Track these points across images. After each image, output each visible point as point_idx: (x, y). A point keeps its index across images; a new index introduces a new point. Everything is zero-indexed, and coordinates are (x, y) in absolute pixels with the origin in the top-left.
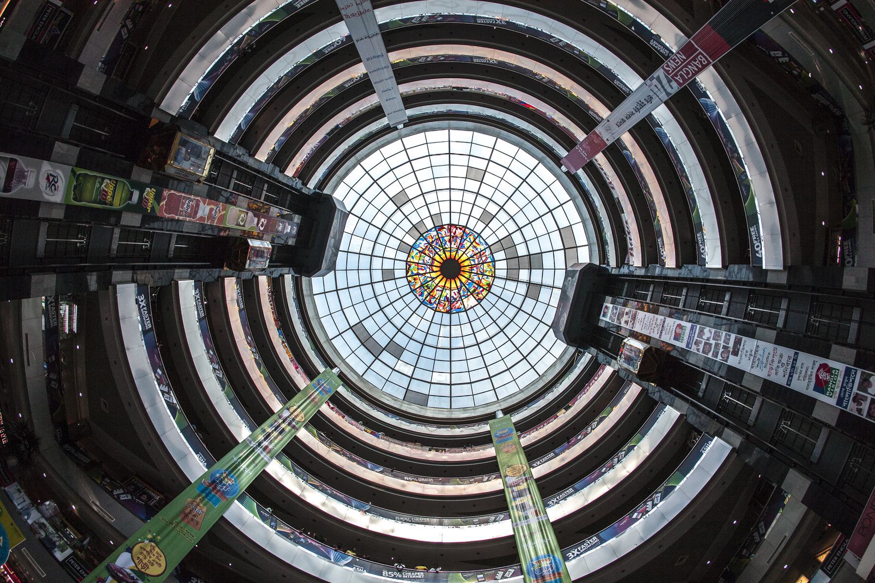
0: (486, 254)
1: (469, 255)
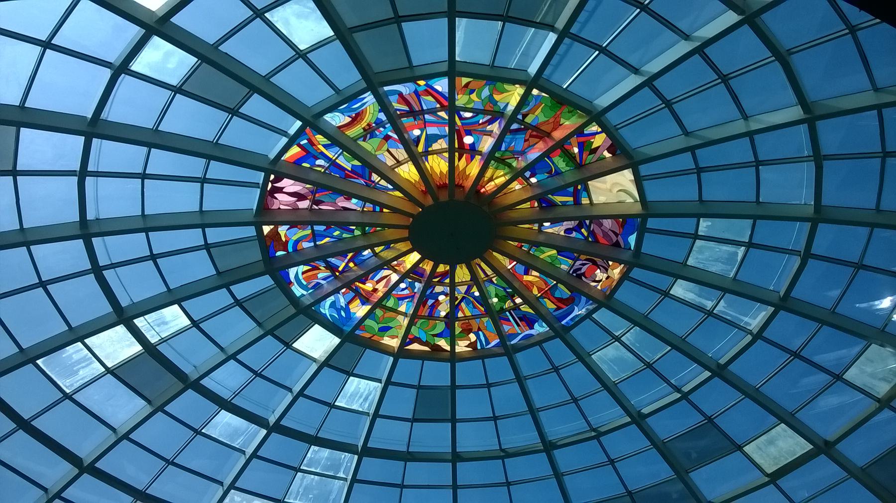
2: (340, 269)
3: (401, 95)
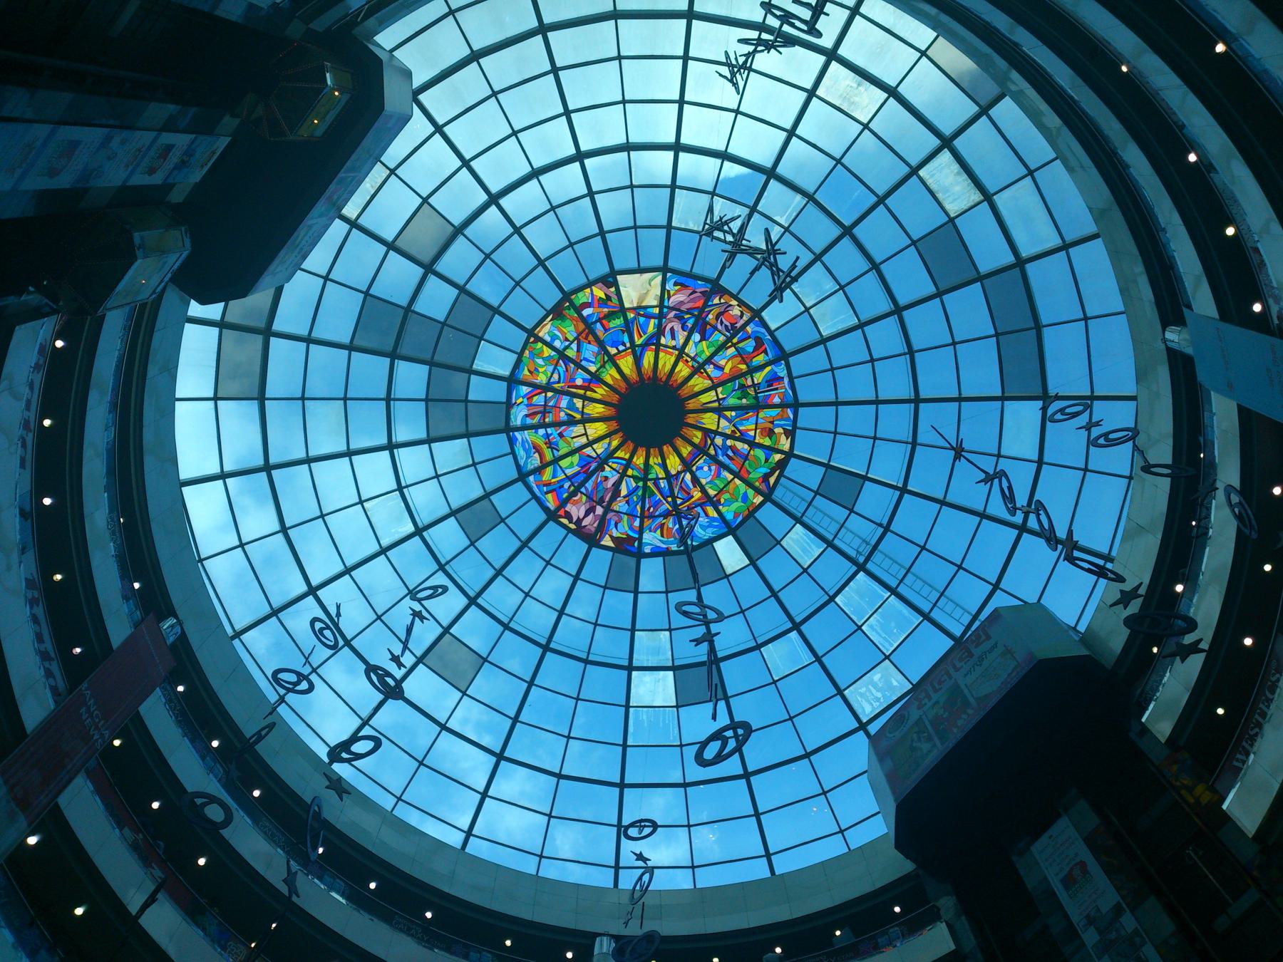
0: (525, 412)
1: (579, 429)
2: (670, 509)
3: (527, 416)
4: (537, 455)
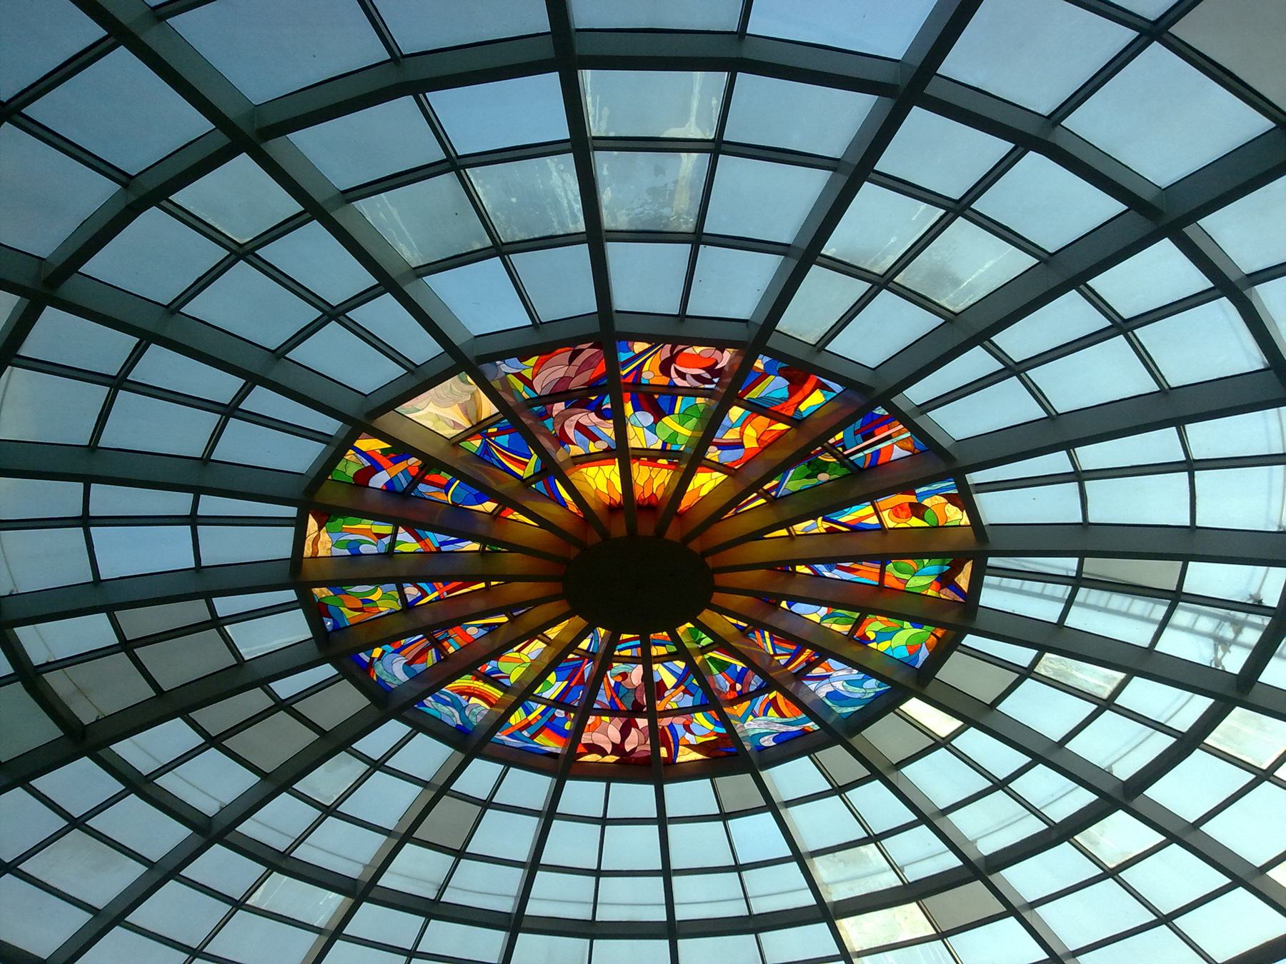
3: (409, 664)
4: (473, 700)
